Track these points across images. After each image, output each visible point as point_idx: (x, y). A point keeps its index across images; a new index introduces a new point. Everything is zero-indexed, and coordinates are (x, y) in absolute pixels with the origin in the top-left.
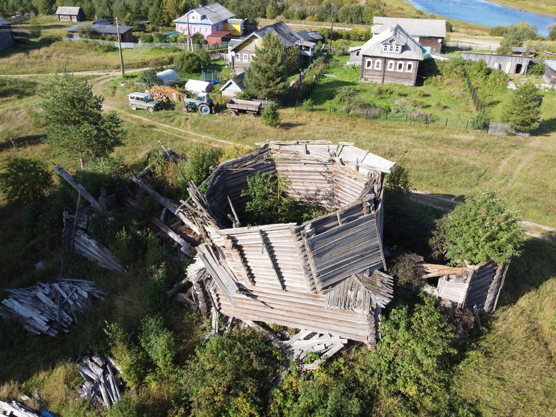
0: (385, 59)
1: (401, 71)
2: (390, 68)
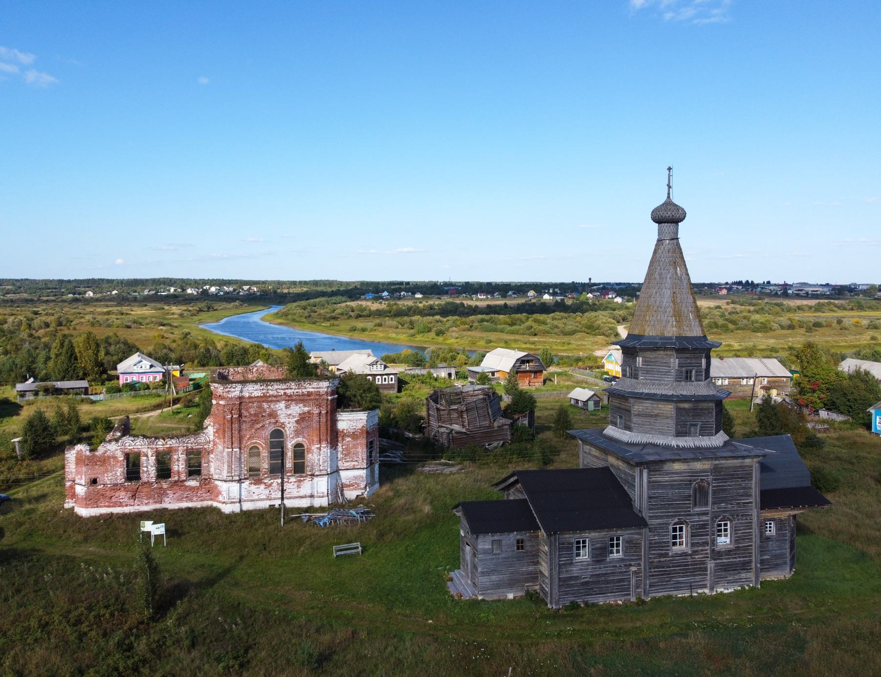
0: (374, 376)
1: (387, 383)
2: (378, 381)
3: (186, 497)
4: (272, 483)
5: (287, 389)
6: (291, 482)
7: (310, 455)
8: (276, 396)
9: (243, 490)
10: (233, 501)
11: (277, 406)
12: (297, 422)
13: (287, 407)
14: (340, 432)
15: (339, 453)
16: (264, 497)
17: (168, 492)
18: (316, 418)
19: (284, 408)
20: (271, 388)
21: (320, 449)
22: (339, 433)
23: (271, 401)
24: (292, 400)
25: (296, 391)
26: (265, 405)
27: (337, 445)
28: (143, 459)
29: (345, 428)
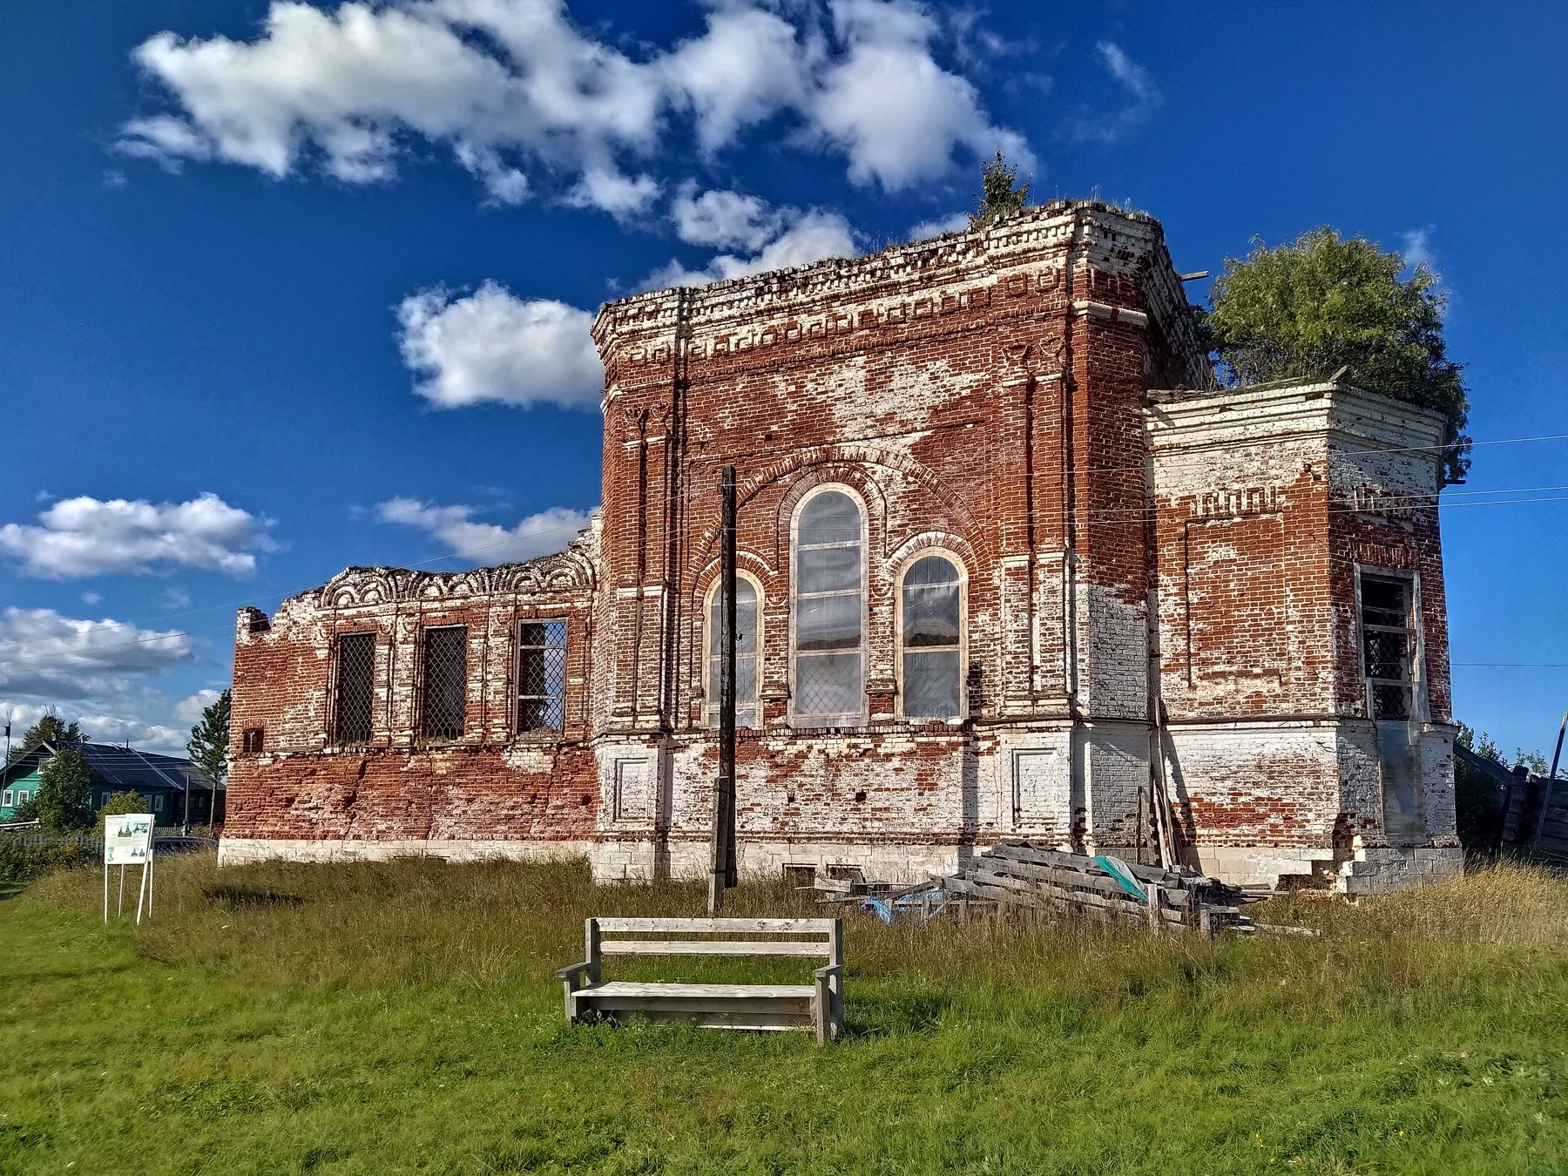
3: (509, 818)
4: (802, 756)
5: (873, 292)
6: (888, 757)
7: (983, 617)
8: (822, 338)
9: (678, 783)
10: (631, 827)
11: (832, 382)
12: (920, 451)
13: (875, 383)
14: (1171, 513)
15: (1163, 628)
16: (766, 824)
17: (453, 792)
18: (1014, 419)
19: (860, 389)
20: (802, 298)
21: (1028, 575)
22: (1162, 521)
23: (806, 363)
24: (898, 345)
25: (918, 296)
26: (781, 385)
27: (1154, 585)
28: (382, 650)
29: (1199, 492)
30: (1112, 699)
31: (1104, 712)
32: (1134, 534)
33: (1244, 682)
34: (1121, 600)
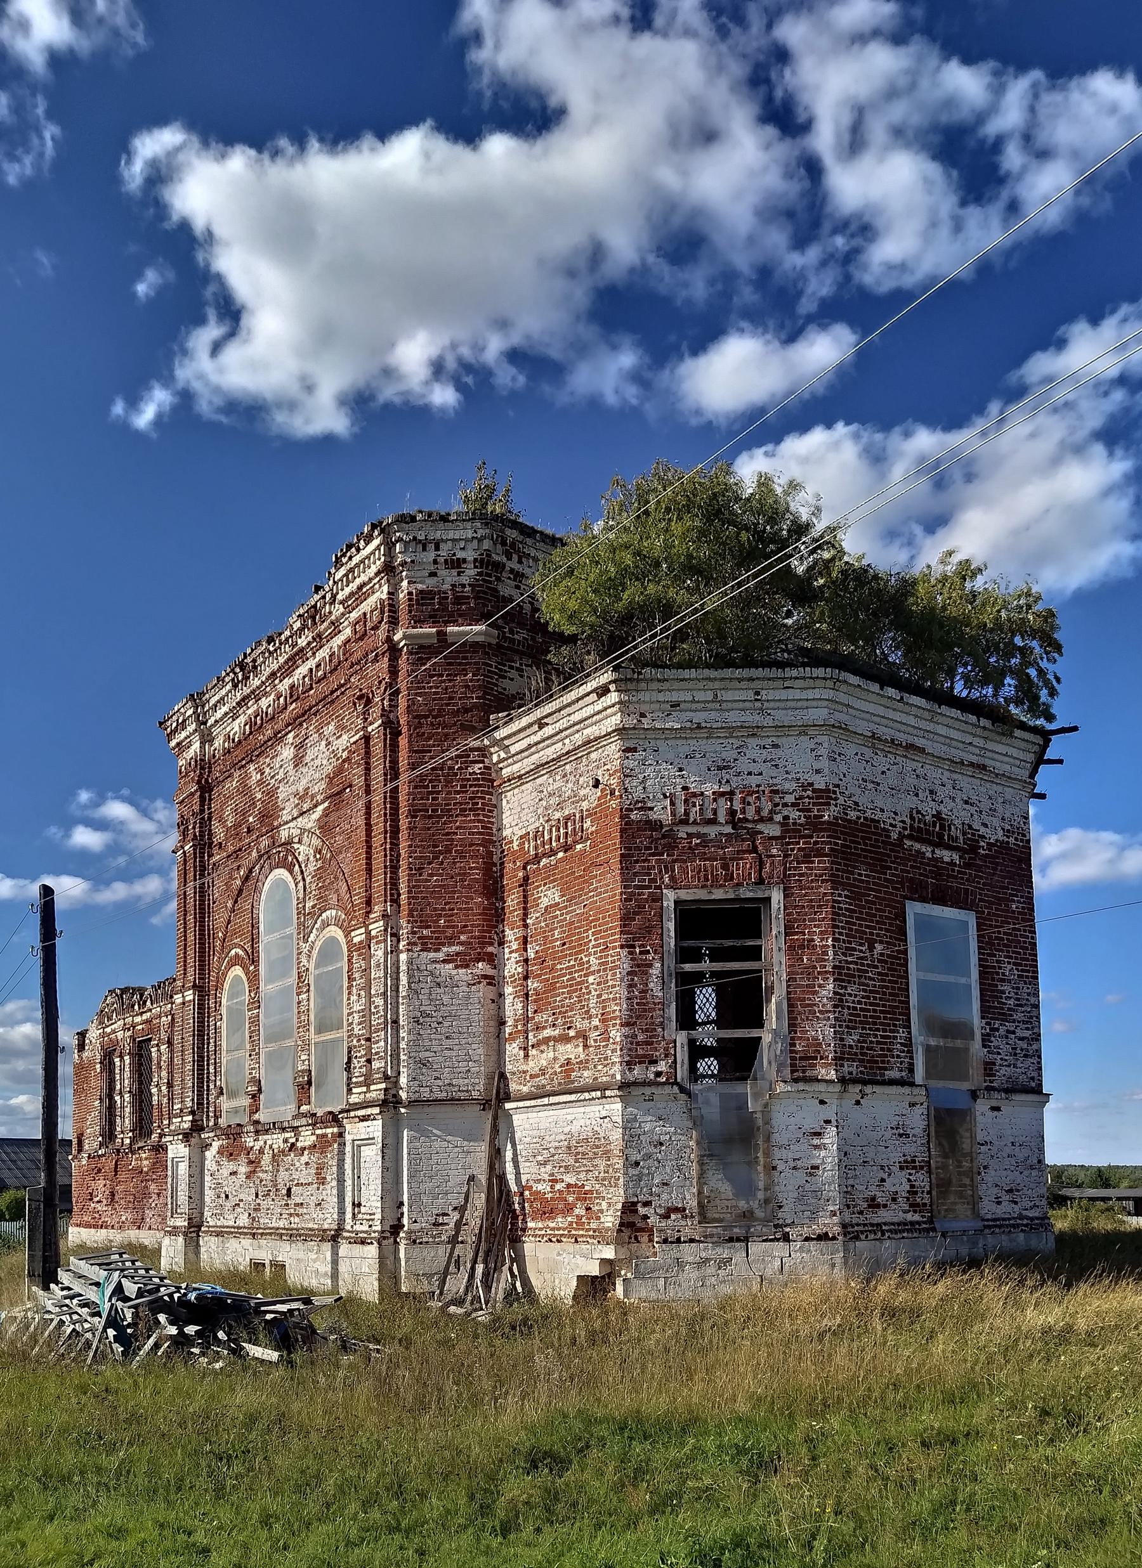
30: (437, 1078)
31: (425, 1094)
32: (470, 887)
33: (561, 1048)
34: (451, 966)
